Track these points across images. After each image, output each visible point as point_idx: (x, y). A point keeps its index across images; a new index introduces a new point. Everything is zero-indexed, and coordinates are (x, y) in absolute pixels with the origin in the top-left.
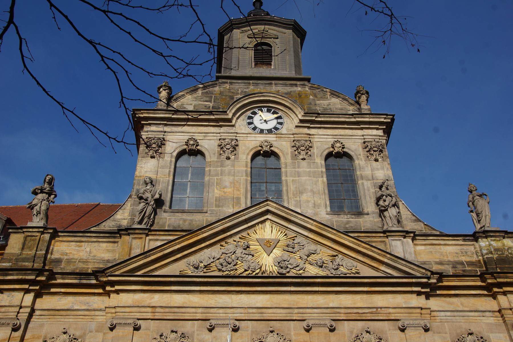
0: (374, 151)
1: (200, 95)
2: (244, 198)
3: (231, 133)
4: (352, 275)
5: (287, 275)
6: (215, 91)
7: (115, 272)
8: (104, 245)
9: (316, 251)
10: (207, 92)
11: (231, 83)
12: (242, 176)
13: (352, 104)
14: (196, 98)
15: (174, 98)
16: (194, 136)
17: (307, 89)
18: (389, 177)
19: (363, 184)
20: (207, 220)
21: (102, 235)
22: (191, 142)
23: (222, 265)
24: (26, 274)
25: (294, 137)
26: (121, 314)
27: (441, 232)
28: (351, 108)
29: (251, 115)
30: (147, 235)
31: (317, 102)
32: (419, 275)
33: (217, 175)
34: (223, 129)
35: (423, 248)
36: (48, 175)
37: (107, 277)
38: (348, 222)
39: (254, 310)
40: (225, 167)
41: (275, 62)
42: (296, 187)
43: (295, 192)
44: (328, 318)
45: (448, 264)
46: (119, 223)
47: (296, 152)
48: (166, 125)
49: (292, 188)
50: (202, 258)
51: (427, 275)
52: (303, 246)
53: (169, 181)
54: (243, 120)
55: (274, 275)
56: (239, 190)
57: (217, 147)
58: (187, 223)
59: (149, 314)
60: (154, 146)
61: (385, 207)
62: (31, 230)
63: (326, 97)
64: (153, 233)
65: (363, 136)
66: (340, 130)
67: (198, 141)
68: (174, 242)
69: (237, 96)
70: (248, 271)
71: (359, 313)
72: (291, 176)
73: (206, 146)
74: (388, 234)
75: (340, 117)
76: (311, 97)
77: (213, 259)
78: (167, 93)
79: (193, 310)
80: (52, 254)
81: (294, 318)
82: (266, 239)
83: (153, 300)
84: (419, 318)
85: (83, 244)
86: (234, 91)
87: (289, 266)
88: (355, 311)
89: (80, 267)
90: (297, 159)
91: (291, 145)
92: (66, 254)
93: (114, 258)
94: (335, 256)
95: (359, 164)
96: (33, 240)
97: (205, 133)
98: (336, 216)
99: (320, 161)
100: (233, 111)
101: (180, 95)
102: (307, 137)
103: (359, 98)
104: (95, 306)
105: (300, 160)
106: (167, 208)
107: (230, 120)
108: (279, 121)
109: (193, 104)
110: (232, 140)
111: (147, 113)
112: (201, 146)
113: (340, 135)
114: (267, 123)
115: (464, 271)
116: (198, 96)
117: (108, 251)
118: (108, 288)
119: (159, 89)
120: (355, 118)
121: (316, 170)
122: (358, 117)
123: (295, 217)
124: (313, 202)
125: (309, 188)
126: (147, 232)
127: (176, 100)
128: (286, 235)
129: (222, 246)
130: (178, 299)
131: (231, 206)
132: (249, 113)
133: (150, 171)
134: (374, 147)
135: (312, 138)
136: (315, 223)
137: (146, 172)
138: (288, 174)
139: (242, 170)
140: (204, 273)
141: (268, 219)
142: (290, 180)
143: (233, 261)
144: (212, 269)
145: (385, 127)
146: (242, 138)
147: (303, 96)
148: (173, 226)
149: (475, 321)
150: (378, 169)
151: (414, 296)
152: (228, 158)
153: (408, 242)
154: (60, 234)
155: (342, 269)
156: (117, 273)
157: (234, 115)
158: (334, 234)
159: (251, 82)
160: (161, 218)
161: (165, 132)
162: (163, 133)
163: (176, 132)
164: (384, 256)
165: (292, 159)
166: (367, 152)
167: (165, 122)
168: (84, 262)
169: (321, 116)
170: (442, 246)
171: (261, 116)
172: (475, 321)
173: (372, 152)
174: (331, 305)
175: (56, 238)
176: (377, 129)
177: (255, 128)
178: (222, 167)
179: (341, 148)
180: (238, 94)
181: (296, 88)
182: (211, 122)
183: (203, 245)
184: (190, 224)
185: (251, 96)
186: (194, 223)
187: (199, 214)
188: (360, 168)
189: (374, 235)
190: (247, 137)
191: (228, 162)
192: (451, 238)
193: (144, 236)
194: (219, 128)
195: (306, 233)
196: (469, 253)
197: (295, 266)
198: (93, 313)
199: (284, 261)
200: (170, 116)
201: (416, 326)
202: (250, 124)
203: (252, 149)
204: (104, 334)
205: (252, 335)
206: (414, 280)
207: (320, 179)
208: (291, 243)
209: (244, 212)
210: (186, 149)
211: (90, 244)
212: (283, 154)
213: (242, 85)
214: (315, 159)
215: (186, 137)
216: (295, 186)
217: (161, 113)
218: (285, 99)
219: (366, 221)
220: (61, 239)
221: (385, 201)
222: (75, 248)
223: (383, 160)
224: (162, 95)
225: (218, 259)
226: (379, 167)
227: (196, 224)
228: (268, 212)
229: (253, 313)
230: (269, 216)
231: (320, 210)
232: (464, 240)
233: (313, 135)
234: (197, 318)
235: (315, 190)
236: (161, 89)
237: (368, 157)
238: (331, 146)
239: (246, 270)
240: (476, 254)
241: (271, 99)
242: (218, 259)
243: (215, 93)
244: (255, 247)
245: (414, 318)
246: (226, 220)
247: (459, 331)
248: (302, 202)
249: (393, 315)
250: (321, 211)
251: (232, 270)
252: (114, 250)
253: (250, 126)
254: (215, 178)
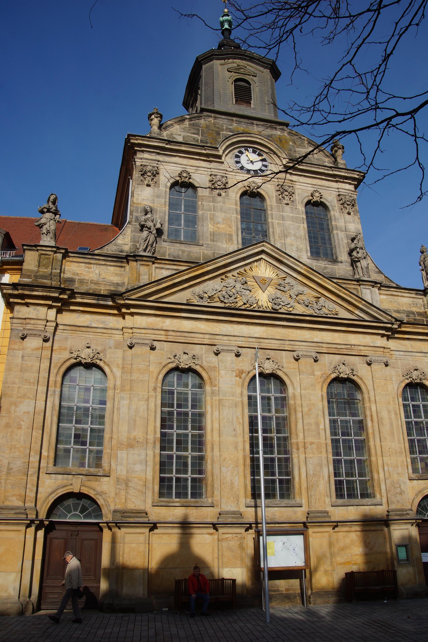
0: (348, 205)
1: (187, 126)
2: (236, 236)
3: (222, 170)
4: (332, 316)
5: (280, 311)
6: (201, 124)
7: (131, 296)
8: (112, 268)
9: (303, 292)
10: (193, 124)
11: (215, 118)
12: (233, 214)
13: (327, 156)
14: (183, 129)
15: (164, 126)
16: (186, 168)
17: (286, 134)
18: (359, 231)
19: (337, 234)
20: (203, 253)
21: (109, 259)
22: (185, 175)
23: (224, 297)
24: (50, 292)
25: (278, 182)
26: (137, 334)
27: (397, 285)
28: (327, 159)
29: (238, 154)
30: (154, 263)
31: (296, 149)
32: (385, 321)
33: (210, 210)
34: (213, 165)
35: (385, 297)
36: (52, 194)
37: (124, 300)
38: (325, 268)
39: (253, 340)
40: (217, 203)
41: (254, 101)
42: (281, 230)
43: (280, 235)
44: (313, 350)
45: (403, 313)
46: (121, 248)
47: (280, 196)
48: (158, 154)
49: (278, 230)
50: (206, 290)
51: (392, 321)
52: (292, 286)
53: (165, 210)
54: (231, 158)
55: (268, 310)
56: (230, 227)
57: (208, 182)
58: (185, 254)
59: (163, 336)
60: (149, 174)
61: (358, 259)
62: (44, 248)
63: (304, 145)
64: (159, 261)
65: (338, 189)
66: (318, 180)
67: (191, 174)
68: (183, 273)
69: (223, 133)
70: (246, 304)
71: (337, 348)
72: (277, 219)
73: (198, 180)
74: (361, 283)
75: (320, 168)
76: (291, 143)
77: (216, 290)
78: (159, 121)
79: (201, 336)
80: (64, 273)
81: (286, 349)
82: (261, 277)
83: (165, 324)
84: (382, 355)
85: (92, 266)
86: (219, 127)
87: (282, 303)
88: (335, 346)
89: (92, 288)
90: (281, 203)
91: (275, 189)
92: (78, 274)
93: (122, 282)
94: (319, 298)
95: (334, 215)
96: (47, 258)
97: (196, 167)
98: (316, 261)
99: (301, 208)
100: (223, 148)
101: (169, 124)
102: (290, 183)
103: (336, 151)
104: (111, 325)
105: (283, 204)
106: (166, 238)
107: (220, 157)
108: (265, 163)
109: (182, 135)
110: (223, 177)
111: (142, 140)
112: (194, 179)
113: (319, 185)
114: (253, 164)
115: (415, 319)
116: (185, 127)
117: (116, 274)
118: (124, 310)
119: (150, 115)
120: (332, 171)
121: (298, 216)
122: (336, 171)
123: (287, 259)
124: (296, 246)
125: (293, 232)
126: (153, 260)
127: (165, 128)
128: (277, 275)
129: (223, 280)
130: (187, 325)
131: (224, 242)
132: (236, 152)
133: (147, 200)
134: (348, 201)
135: (294, 184)
136: (304, 267)
137: (143, 199)
138: (274, 217)
139: (232, 208)
140: (208, 303)
141: (262, 258)
142: (275, 222)
143: (234, 294)
144: (215, 300)
145: (356, 183)
146: (231, 176)
147: (283, 141)
148: (173, 256)
149: (420, 360)
150: (350, 222)
151: (379, 337)
152: (220, 195)
153: (375, 292)
154: (70, 254)
155: (324, 309)
156: (133, 297)
157: (224, 151)
158: (320, 279)
159: (234, 119)
160: (161, 247)
161: (159, 161)
162: (157, 162)
163: (169, 163)
164: (360, 302)
165: (277, 203)
166: (341, 204)
167: (158, 151)
168: (96, 283)
169: (303, 164)
170: (399, 298)
171: (247, 156)
172: (420, 360)
173: (346, 206)
174: (315, 340)
175: (67, 258)
176: (350, 184)
177: (242, 168)
178: (215, 203)
179: (319, 198)
180: (223, 130)
181: (275, 131)
182: (202, 157)
183: (206, 277)
184: (188, 255)
185: (239, 135)
186: (192, 255)
187: (196, 246)
188: (335, 219)
189: (349, 282)
190: (236, 175)
191: (219, 198)
192: (407, 291)
193: (150, 263)
194: (209, 163)
195: (295, 275)
196: (418, 305)
197: (287, 303)
198: (110, 331)
199: (277, 298)
200: (164, 145)
201: (379, 362)
202: (238, 162)
203: (240, 188)
204: (124, 351)
205: (251, 361)
206: (382, 325)
207: (302, 225)
208: (282, 283)
209: (244, 251)
210: (178, 181)
211: (98, 266)
212: (269, 197)
213: (225, 121)
214: (297, 206)
215: (179, 169)
216: (280, 229)
217: (155, 141)
218: (271, 143)
219: (340, 269)
220: (71, 259)
221: (358, 253)
222: (84, 269)
223: (354, 214)
224: (153, 122)
225: (220, 291)
226: (351, 220)
227: (194, 256)
228: (263, 252)
229: (252, 342)
230: (263, 256)
231: (302, 254)
232: (416, 294)
233: (295, 182)
234: (205, 343)
235: (297, 235)
236: (153, 117)
237: (342, 209)
238: (310, 195)
239: (245, 304)
240: (424, 307)
241: (258, 140)
242: (220, 291)
243: (202, 126)
244: (251, 283)
245: (378, 355)
246: (228, 256)
247: (408, 367)
248: (286, 245)
249: (363, 351)
250: (303, 255)
251: (233, 303)
252: (121, 274)
253: (238, 165)
254: (209, 212)
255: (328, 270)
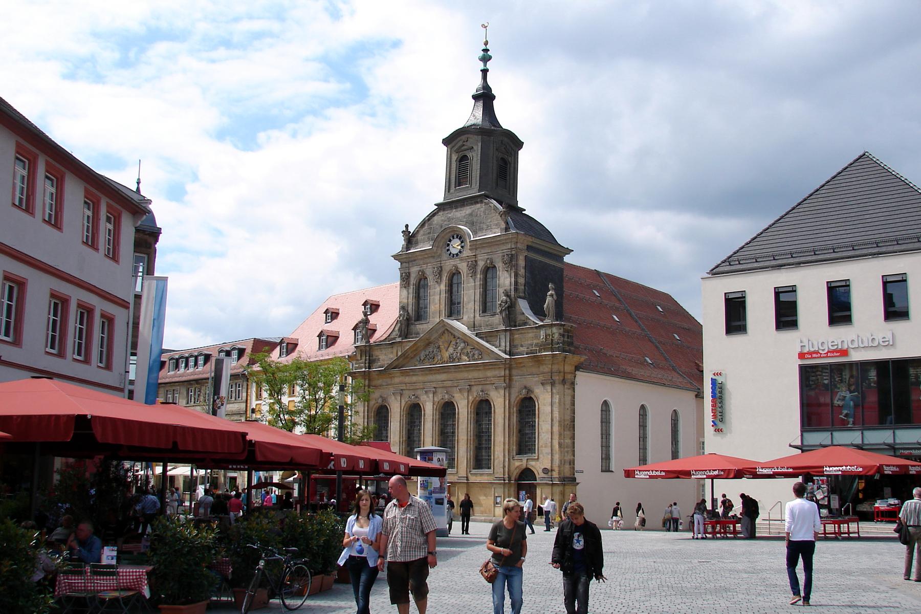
38: (489, 321)
80: (372, 357)
255: (490, 322)
